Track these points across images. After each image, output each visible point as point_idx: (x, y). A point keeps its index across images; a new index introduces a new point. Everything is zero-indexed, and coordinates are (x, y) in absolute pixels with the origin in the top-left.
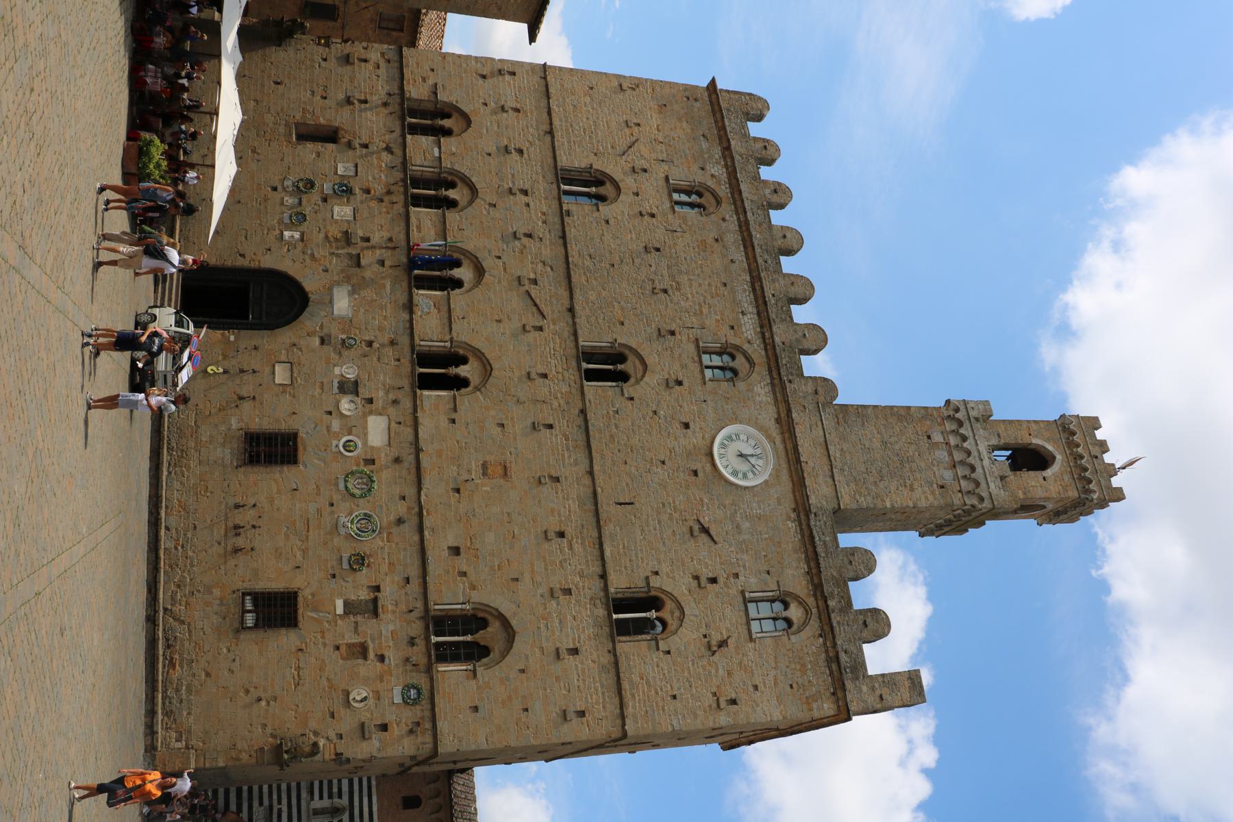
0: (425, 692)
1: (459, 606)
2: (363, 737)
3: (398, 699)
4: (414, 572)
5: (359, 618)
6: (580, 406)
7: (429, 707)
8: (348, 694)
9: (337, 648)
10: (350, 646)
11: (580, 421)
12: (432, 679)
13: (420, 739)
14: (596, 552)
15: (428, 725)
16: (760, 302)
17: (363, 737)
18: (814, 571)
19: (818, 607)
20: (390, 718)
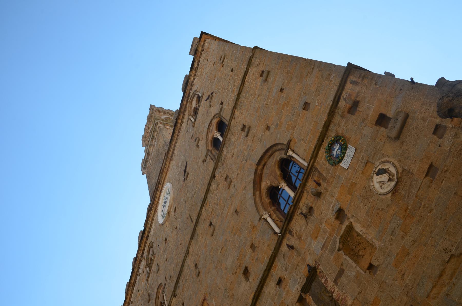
0: (326, 144)
1: (269, 220)
2: (407, 116)
3: (350, 151)
4: (271, 285)
5: (330, 285)
6: (174, 300)
7: (332, 127)
8: (394, 191)
9: (371, 267)
10: (356, 257)
11: (177, 292)
12: (314, 156)
13: (357, 88)
14: (210, 196)
15: (342, 104)
16: (135, 272)
17: (407, 116)
18: (180, 121)
19: (187, 101)
20: (368, 130)
